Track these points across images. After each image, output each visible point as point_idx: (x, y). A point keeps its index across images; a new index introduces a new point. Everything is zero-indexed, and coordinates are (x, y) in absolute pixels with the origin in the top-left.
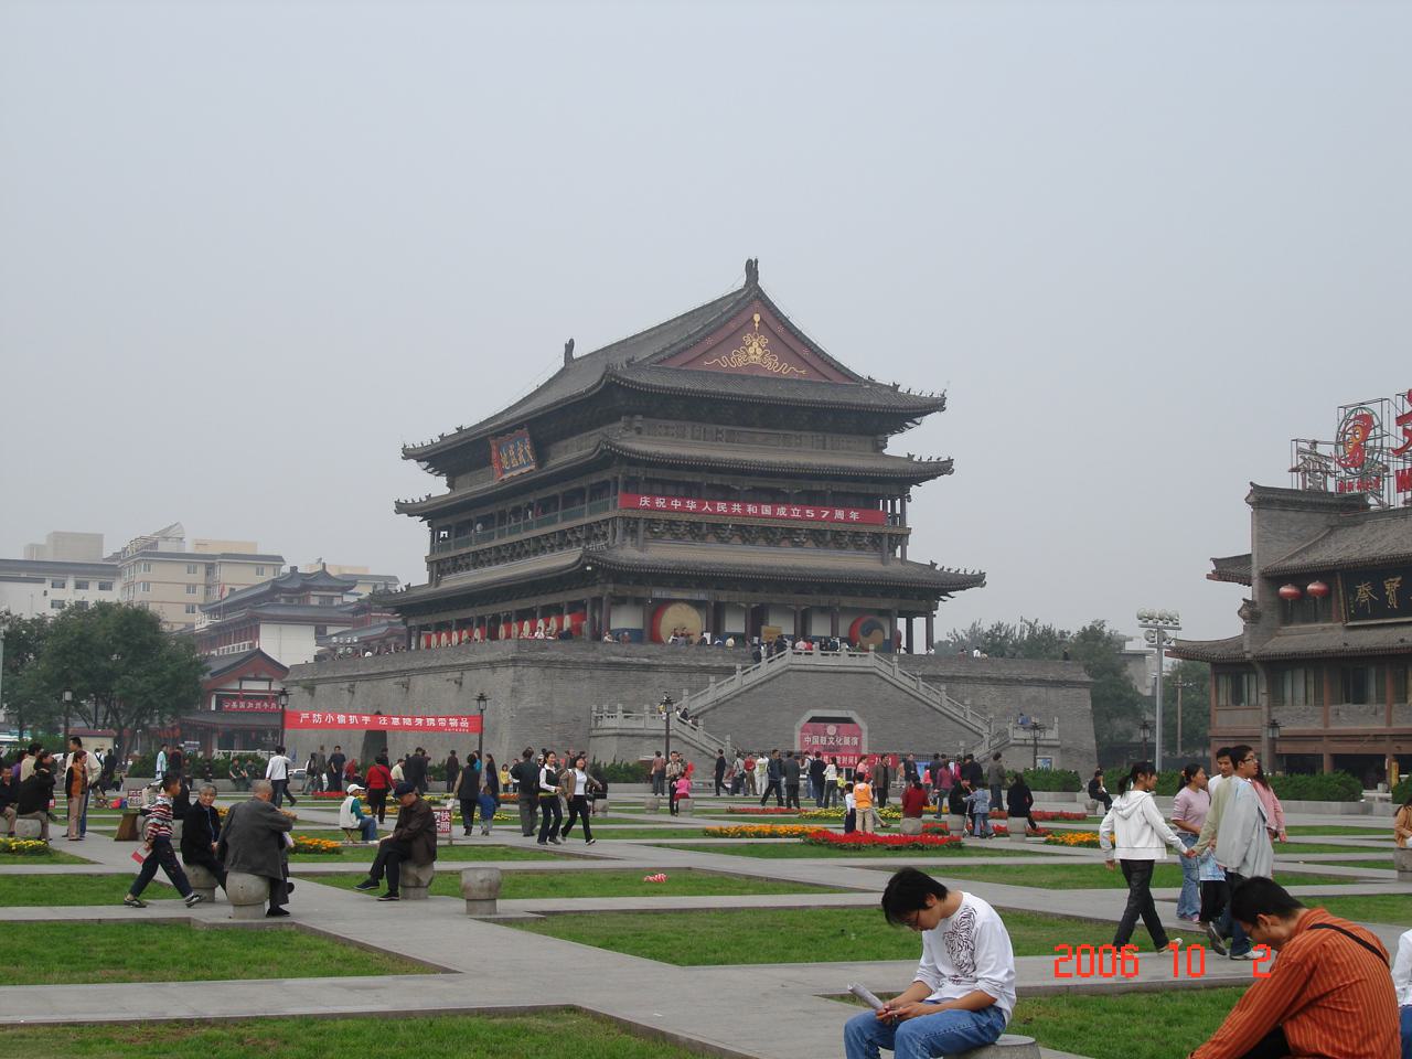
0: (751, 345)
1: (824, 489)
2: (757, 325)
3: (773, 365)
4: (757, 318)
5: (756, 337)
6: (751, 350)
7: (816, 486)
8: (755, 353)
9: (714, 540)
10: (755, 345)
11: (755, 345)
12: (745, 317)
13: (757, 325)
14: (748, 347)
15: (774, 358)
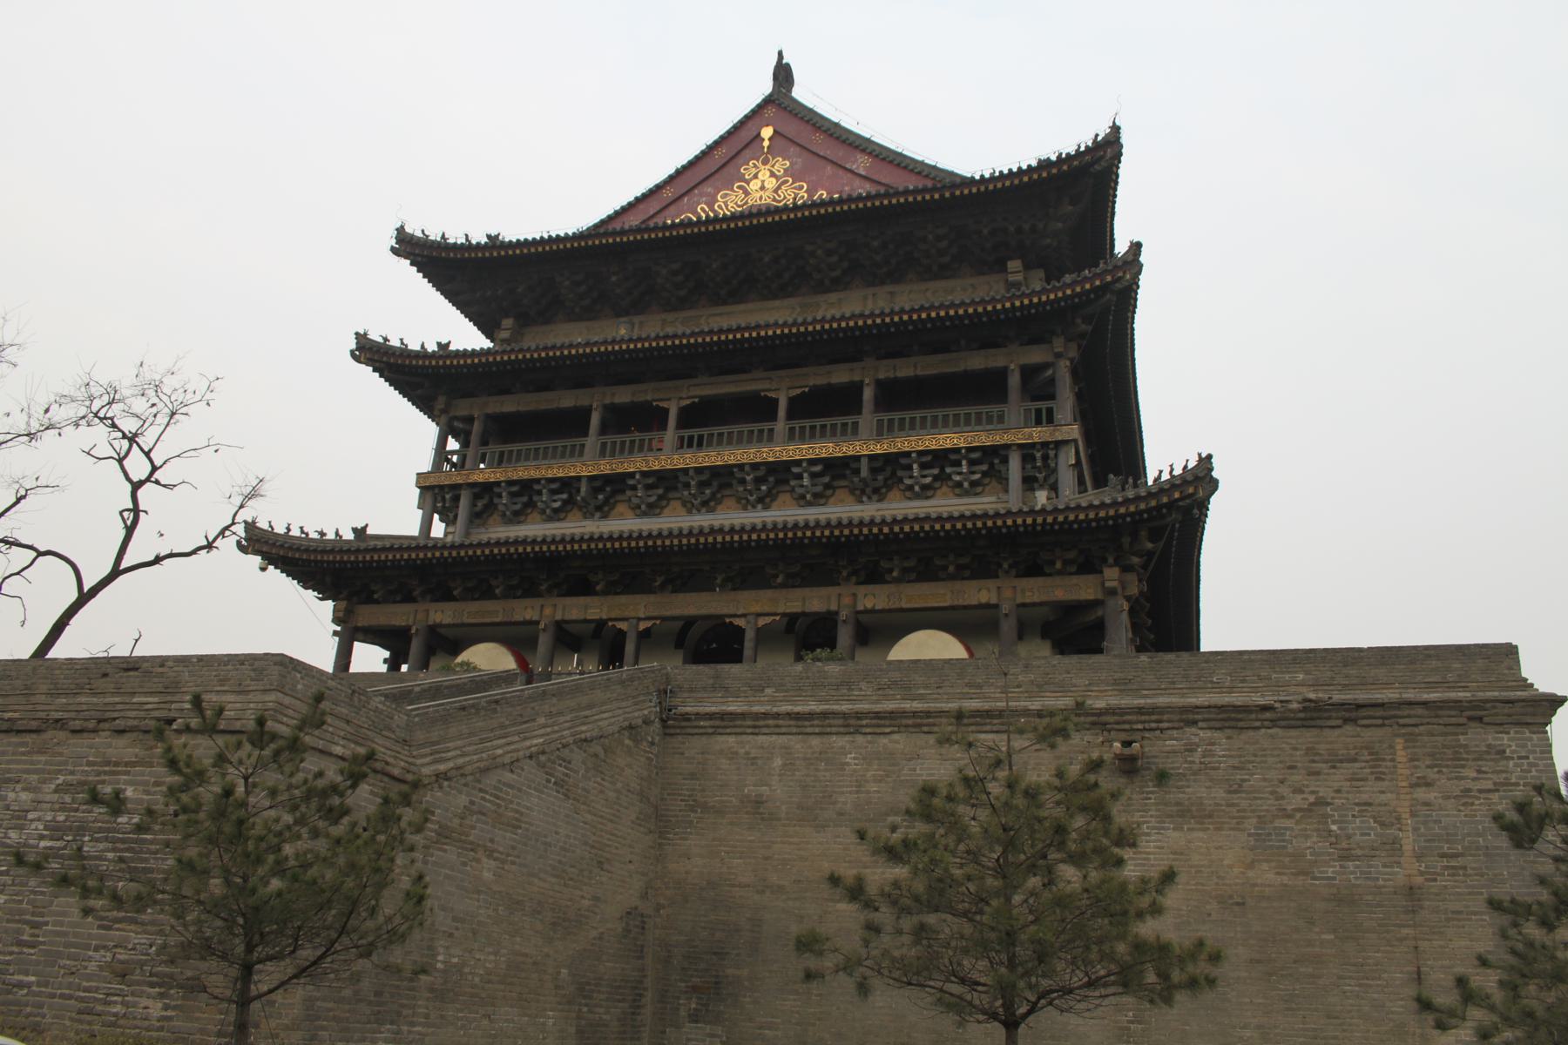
0: (756, 177)
1: (857, 378)
2: (766, 144)
3: (794, 194)
4: (767, 132)
5: (765, 162)
6: (754, 185)
7: (840, 375)
8: (763, 188)
9: (630, 513)
10: (764, 174)
11: (764, 174)
12: (745, 135)
13: (766, 144)
14: (748, 182)
15: (801, 188)
